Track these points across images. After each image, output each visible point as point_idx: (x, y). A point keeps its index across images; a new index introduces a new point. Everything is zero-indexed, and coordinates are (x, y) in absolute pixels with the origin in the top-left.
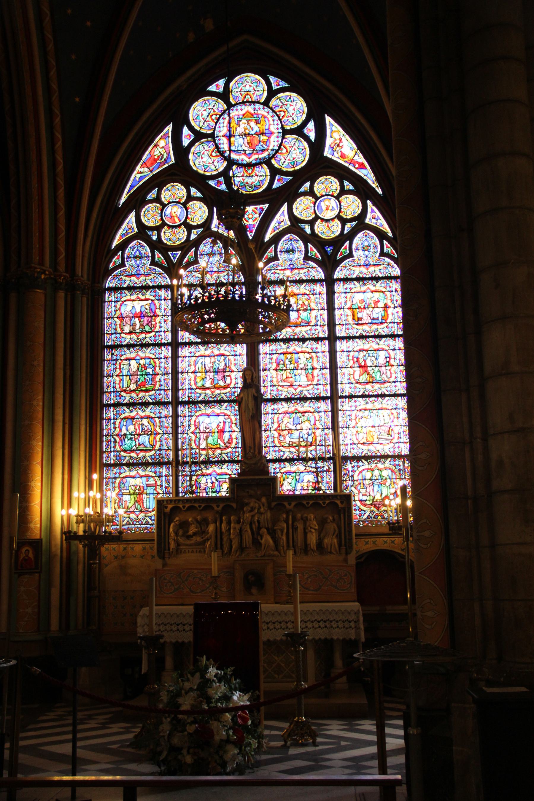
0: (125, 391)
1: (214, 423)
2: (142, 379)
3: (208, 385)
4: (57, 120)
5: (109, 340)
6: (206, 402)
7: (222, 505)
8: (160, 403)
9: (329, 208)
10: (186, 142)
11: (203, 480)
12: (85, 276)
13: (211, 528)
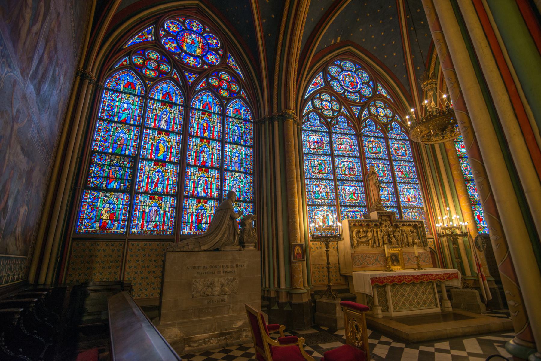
1: (351, 189)
2: (320, 169)
3: (347, 173)
5: (305, 151)
6: (347, 181)
7: (374, 224)
8: (329, 179)
9: (382, 112)
11: (350, 214)
13: (370, 235)
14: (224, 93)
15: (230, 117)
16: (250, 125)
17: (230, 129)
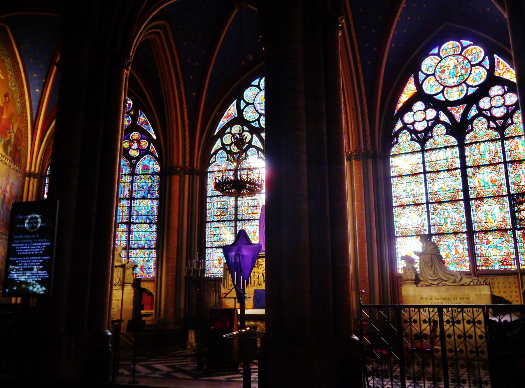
0: (215, 215)
2: (222, 210)
3: (250, 212)
4: (185, 104)
6: (249, 220)
8: (229, 221)
10: (242, 107)
12: (198, 167)
14: (134, 153)
15: (138, 175)
16: (157, 177)
17: (138, 186)
